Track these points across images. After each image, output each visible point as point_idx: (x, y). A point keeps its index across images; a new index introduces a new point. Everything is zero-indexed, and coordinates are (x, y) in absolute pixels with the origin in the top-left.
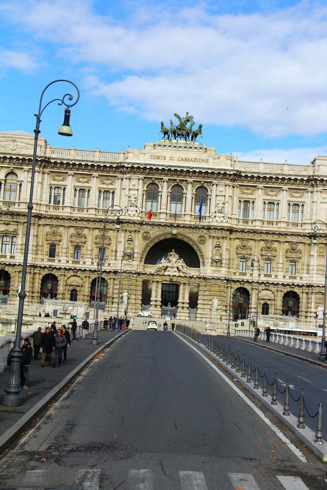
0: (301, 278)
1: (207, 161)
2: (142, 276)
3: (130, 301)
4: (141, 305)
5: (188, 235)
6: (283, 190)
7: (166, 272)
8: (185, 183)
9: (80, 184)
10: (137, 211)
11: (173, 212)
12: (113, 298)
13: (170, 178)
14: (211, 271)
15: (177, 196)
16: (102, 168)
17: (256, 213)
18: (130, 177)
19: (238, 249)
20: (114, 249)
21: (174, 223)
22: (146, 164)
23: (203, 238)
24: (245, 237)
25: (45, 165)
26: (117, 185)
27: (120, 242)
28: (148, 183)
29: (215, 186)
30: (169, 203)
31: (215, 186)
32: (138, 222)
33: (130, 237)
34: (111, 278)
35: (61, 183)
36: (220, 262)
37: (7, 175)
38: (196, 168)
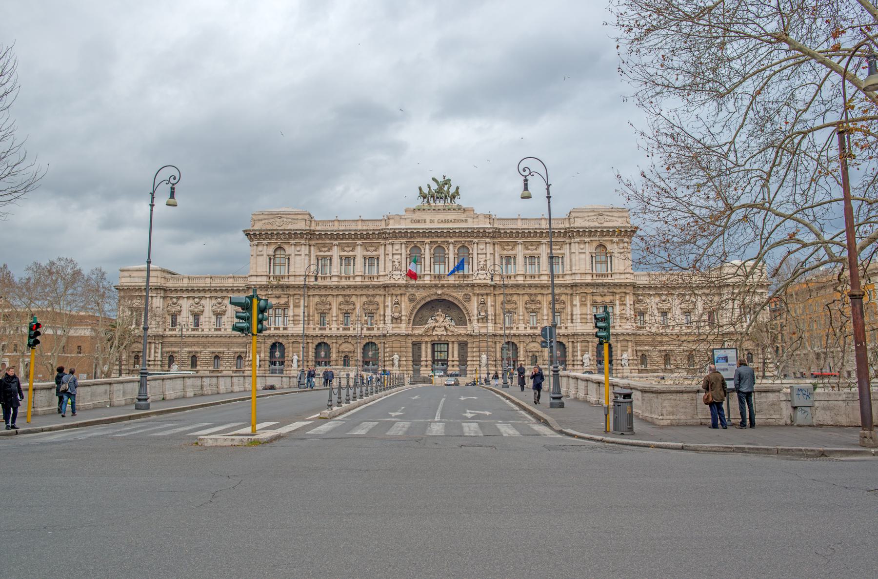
0: (566, 328)
1: (466, 221)
9: (345, 253)
11: (437, 273)
15: (439, 256)
20: (382, 313)
26: (381, 251)
35: (327, 253)
37: (276, 250)
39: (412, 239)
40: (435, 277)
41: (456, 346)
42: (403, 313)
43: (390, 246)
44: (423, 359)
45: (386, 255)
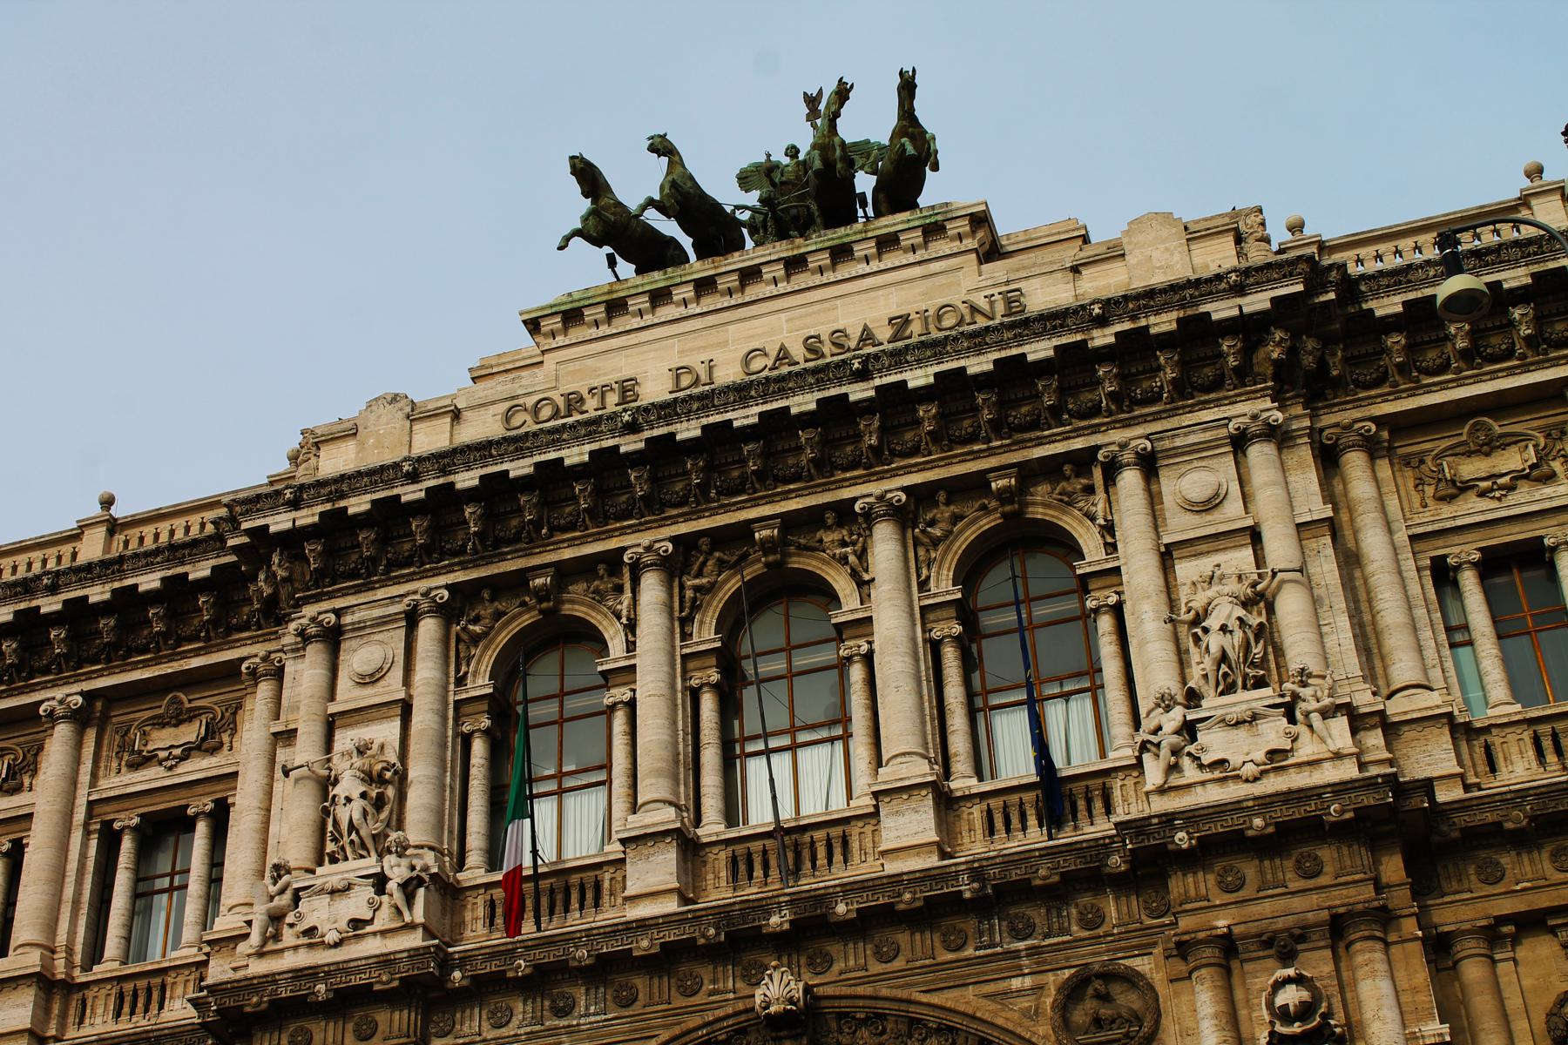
5: (935, 999)
10: (380, 882)
13: (683, 528)
21: (762, 907)
23: (1128, 1000)
28: (503, 638)
29: (1130, 479)
31: (1130, 479)
32: (384, 980)
39: (483, 540)
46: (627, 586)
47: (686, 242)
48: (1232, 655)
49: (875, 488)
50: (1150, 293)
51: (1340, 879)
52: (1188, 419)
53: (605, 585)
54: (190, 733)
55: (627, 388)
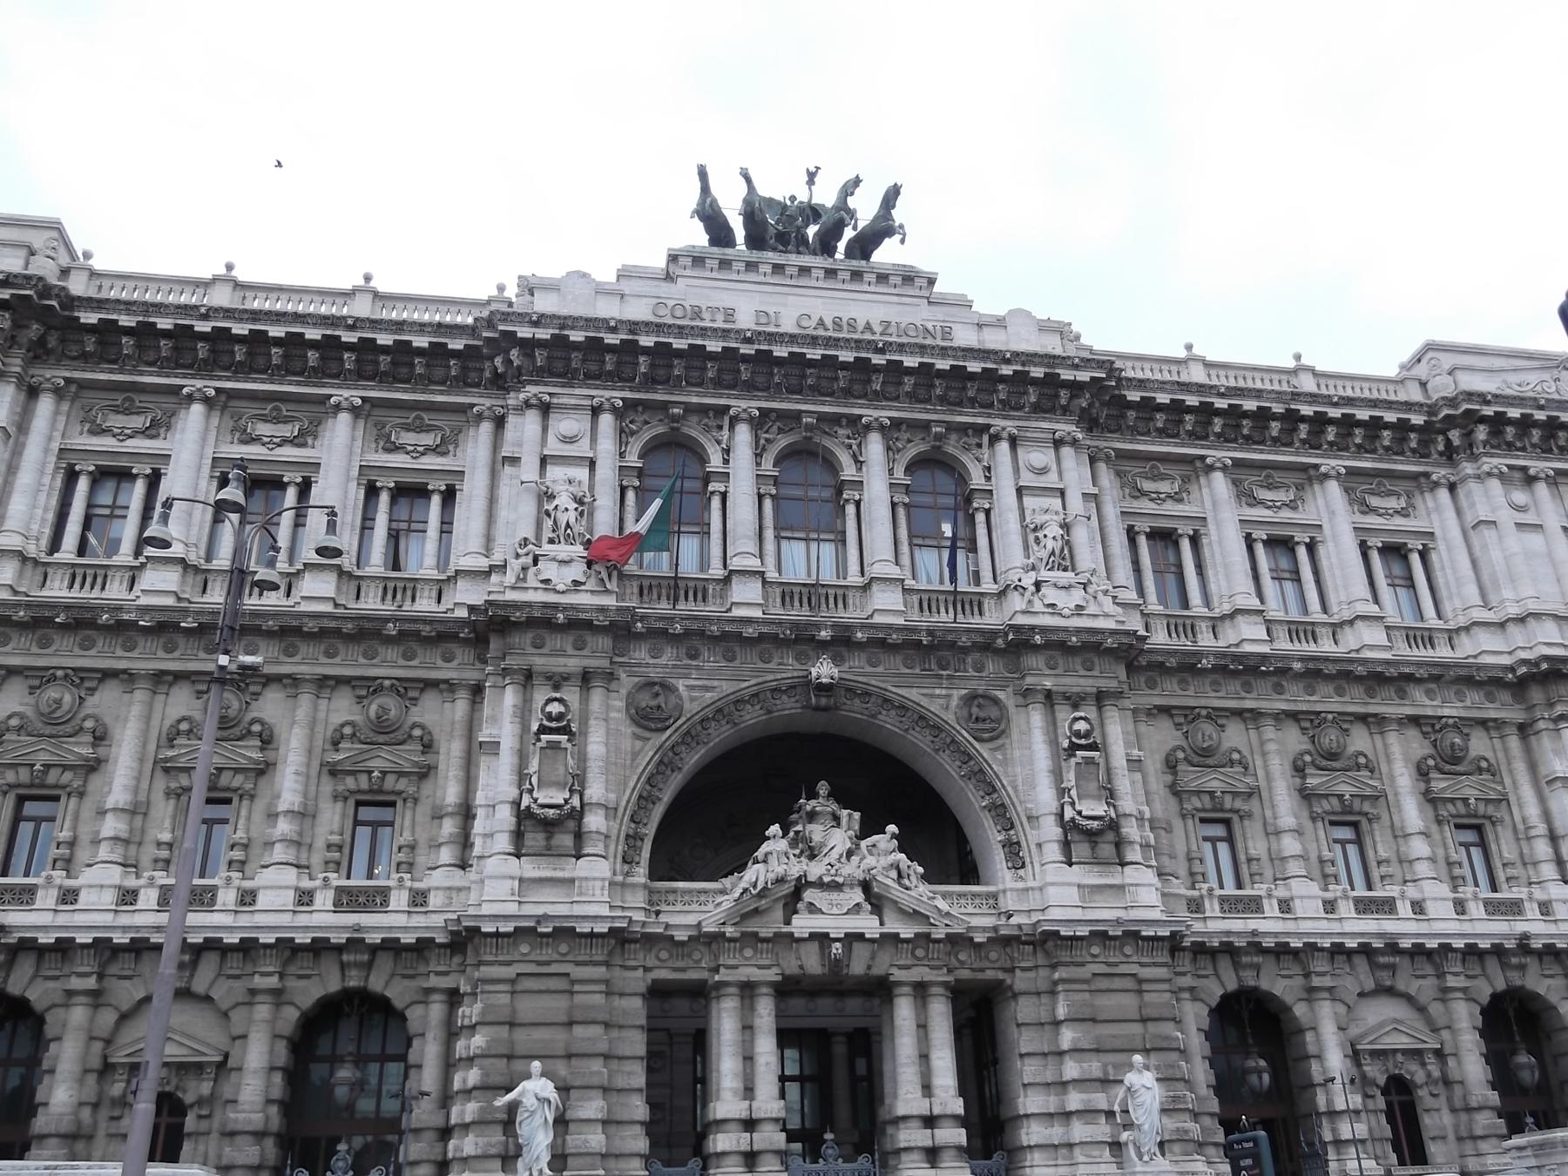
2: (638, 956)
3: (574, 1141)
4: (647, 1159)
5: (899, 691)
6: (1326, 476)
7: (797, 921)
8: (849, 432)
12: (445, 1133)
14: (1073, 896)
15: (809, 490)
16: (385, 360)
17: (1223, 583)
18: (547, 398)
19: (1182, 767)
20: (451, 794)
21: (818, 626)
22: (634, 327)
23: (994, 712)
24: (1203, 702)
25: (42, 341)
26: (475, 450)
27: (493, 747)
29: (1004, 447)
30: (769, 534)
31: (1004, 447)
32: (601, 620)
33: (555, 708)
34: (428, 991)
36: (1110, 836)
38: (901, 348)
40: (788, 593)
41: (940, 1015)
42: (595, 790)
43: (532, 420)
44: (727, 1104)
45: (502, 461)
46: (726, 427)
47: (740, 234)
48: (1057, 552)
49: (876, 413)
50: (1035, 355)
51: (1111, 676)
52: (1035, 424)
53: (713, 423)
54: (428, 439)
55: (729, 314)
